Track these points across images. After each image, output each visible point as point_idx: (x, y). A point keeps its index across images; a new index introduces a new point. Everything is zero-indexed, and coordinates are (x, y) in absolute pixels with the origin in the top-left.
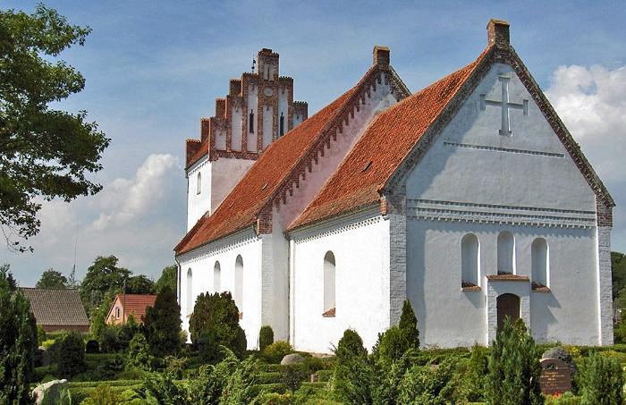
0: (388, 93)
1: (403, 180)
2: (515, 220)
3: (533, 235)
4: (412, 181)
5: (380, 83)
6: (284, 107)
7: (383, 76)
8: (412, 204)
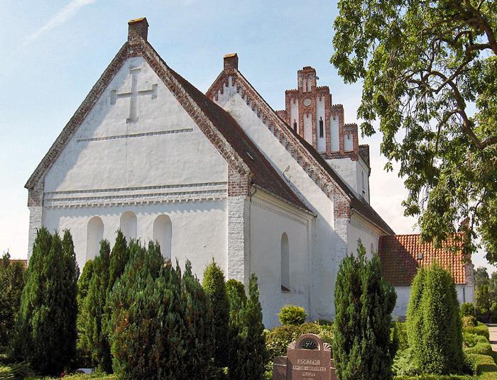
0: (234, 93)
1: (42, 177)
2: (137, 200)
3: (89, 216)
4: (50, 179)
5: (227, 86)
6: (321, 112)
7: (230, 79)
8: (49, 197)
